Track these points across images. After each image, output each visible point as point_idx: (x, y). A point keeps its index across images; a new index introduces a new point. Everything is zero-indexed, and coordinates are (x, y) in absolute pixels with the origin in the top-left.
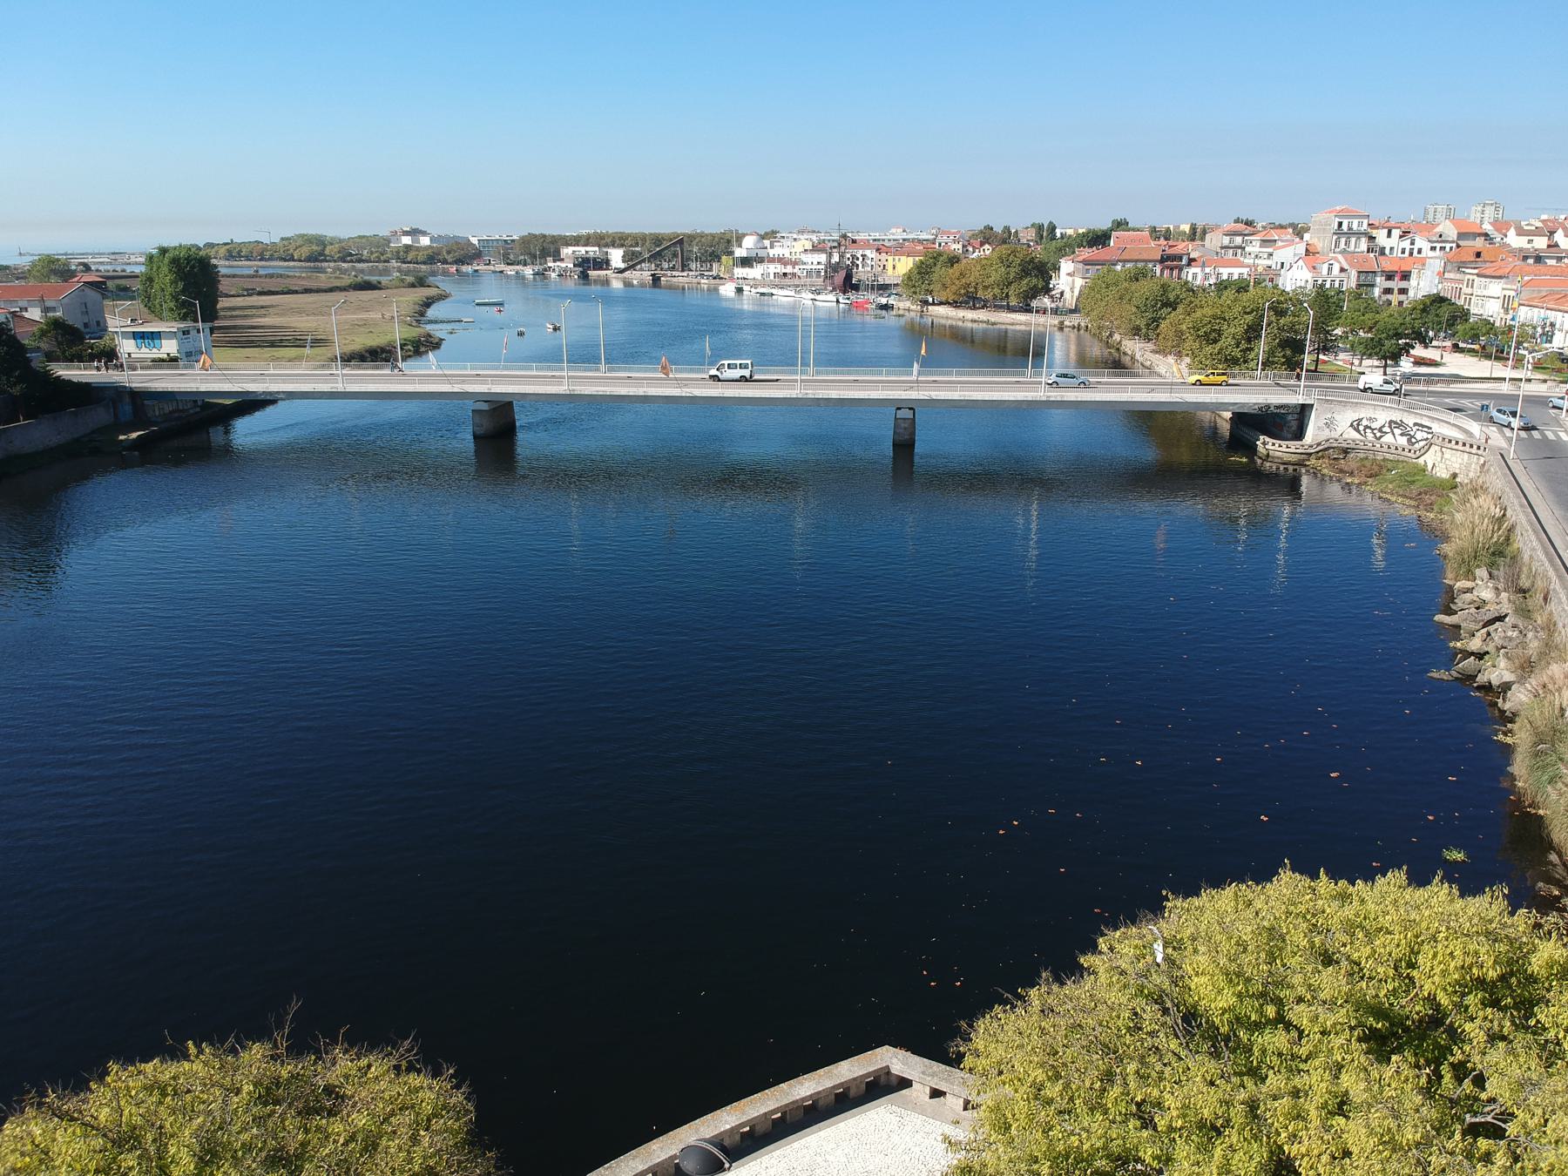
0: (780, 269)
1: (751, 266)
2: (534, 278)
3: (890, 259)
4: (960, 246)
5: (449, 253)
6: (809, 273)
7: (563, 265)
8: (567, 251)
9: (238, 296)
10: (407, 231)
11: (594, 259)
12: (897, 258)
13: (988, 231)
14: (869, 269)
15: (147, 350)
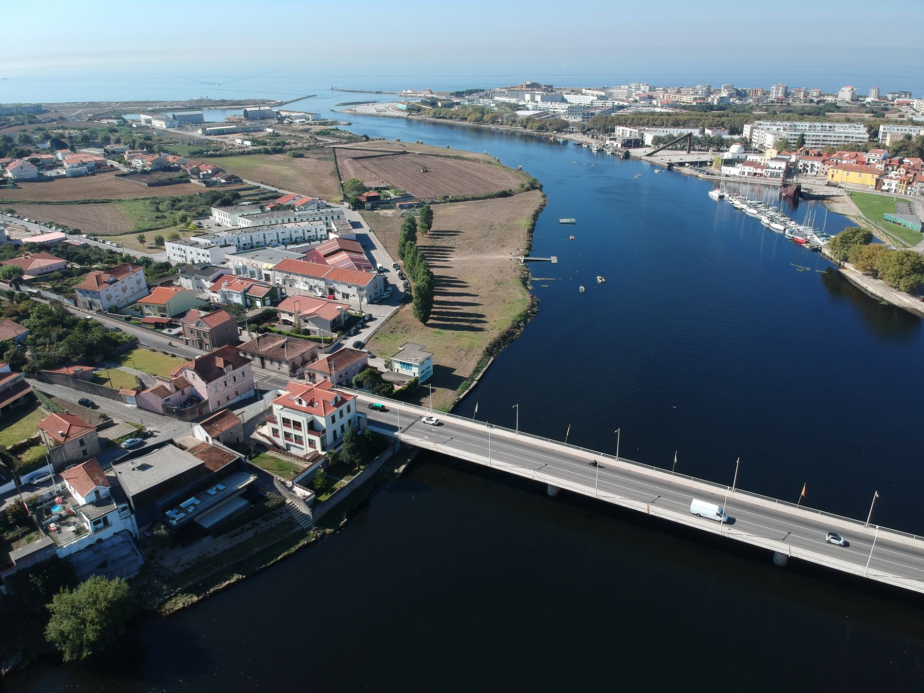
0: (752, 170)
1: (733, 165)
2: (597, 153)
3: (831, 170)
4: (883, 166)
6: (772, 175)
8: (619, 130)
9: (440, 203)
10: (528, 85)
11: (635, 140)
12: (835, 170)
14: (815, 173)
15: (405, 369)
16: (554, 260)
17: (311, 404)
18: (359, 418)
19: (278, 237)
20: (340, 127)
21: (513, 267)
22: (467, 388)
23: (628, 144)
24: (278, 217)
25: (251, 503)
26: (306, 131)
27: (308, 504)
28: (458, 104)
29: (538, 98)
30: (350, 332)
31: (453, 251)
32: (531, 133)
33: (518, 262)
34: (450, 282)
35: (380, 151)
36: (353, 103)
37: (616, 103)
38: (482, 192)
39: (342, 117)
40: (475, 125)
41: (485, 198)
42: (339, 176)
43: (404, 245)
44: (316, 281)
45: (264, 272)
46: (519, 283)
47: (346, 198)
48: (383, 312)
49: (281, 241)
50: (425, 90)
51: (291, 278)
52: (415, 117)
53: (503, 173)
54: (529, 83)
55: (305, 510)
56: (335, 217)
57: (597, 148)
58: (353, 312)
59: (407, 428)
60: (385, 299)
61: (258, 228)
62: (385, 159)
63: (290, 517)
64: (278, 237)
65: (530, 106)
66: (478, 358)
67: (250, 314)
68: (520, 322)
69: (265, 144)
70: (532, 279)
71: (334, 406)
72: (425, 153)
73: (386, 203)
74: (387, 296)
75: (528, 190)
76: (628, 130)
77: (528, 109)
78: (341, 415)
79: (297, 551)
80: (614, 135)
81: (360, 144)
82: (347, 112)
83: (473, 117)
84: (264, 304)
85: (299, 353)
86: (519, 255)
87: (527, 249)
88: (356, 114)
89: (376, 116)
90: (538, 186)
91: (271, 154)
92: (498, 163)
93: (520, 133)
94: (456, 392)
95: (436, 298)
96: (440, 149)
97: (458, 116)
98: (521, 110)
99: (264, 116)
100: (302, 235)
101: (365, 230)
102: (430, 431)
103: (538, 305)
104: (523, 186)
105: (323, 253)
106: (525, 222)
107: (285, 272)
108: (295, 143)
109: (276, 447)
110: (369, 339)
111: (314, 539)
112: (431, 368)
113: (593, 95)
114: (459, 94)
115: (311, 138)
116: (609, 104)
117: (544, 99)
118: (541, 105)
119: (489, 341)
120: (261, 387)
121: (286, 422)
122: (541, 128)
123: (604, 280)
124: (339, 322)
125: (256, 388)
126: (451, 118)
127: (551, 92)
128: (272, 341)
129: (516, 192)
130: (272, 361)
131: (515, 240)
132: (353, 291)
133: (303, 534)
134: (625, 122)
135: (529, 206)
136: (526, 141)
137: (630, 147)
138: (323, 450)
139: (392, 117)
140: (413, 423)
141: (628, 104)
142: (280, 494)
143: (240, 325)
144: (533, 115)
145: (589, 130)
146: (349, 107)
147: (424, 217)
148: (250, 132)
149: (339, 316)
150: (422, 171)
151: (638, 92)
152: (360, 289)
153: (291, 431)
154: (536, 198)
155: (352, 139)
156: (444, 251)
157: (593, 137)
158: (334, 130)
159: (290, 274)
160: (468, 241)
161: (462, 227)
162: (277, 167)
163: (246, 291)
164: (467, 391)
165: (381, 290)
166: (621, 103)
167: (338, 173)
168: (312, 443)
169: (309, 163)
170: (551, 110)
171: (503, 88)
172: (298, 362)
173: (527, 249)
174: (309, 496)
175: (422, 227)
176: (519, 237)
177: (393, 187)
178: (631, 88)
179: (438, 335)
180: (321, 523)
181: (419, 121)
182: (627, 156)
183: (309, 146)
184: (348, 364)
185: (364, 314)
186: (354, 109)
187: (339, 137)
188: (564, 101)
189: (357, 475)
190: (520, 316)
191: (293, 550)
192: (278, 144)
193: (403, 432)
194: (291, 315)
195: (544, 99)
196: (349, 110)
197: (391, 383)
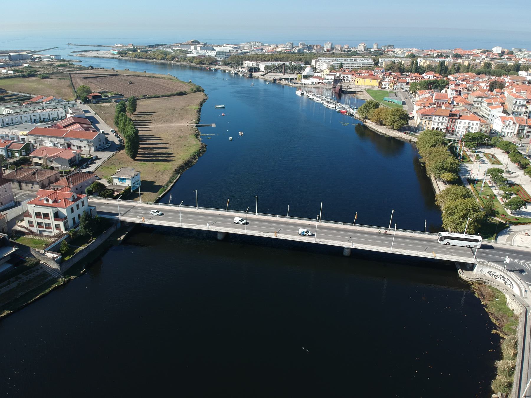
2: (234, 76)
3: (357, 79)
4: (382, 76)
5: (207, 61)
7: (244, 70)
8: (246, 63)
9: (141, 99)
10: (192, 42)
12: (359, 79)
13: (393, 64)
15: (122, 183)
16: (214, 125)
17: (55, 201)
18: (91, 209)
19: (31, 118)
20: (74, 63)
21: (189, 129)
22: (164, 191)
23: (251, 70)
24: (31, 108)
25: (15, 266)
26: (51, 65)
27: (57, 261)
28: (150, 50)
29: (199, 48)
30: (83, 166)
31: (151, 122)
32: (195, 66)
33: (192, 127)
34: (149, 138)
35: (101, 74)
36: (82, 51)
37: (243, 51)
38: (168, 93)
39: (75, 58)
40: (162, 61)
41: (170, 96)
42: (74, 87)
43: (118, 117)
44: (57, 139)
45: (21, 137)
46: (193, 136)
47: (78, 97)
48: (104, 156)
49: (33, 121)
50: (130, 44)
51: (40, 139)
52: (123, 57)
53: (180, 84)
54: (193, 41)
55: (54, 266)
56: (71, 106)
57: (234, 72)
58: (85, 156)
59: (125, 214)
60: (107, 148)
61: (16, 113)
62: (104, 78)
63: (44, 272)
64: (31, 118)
65: (194, 52)
66: (171, 175)
67: (11, 161)
68: (195, 156)
69: (23, 72)
70: (201, 135)
71: (72, 201)
72: (130, 75)
73: (105, 100)
74: (108, 147)
75: (196, 92)
76: (251, 63)
77: (193, 53)
78: (78, 208)
79: (50, 292)
80: (243, 66)
81: (87, 71)
82: (78, 55)
83: (160, 57)
84: (21, 154)
85: (46, 177)
86: (193, 123)
87: (197, 120)
88: (84, 57)
89: (98, 57)
90: (202, 90)
91: (26, 77)
92: (176, 79)
93: (189, 66)
94: (157, 194)
95: (141, 146)
96: (141, 73)
97: (151, 56)
98: (189, 54)
99: (22, 58)
100: (48, 117)
101: (92, 113)
102: (141, 213)
103: (205, 147)
104: (192, 89)
105: (62, 125)
106: (195, 107)
107: (36, 135)
108: (43, 71)
109: (31, 233)
110: (96, 169)
111: (62, 283)
112: (139, 182)
113: (230, 47)
114: (150, 46)
115: (54, 68)
116: (240, 51)
117: (202, 48)
118: (200, 51)
119: (177, 166)
120: (19, 200)
121: (38, 215)
122: (201, 63)
123: (243, 134)
124: (74, 161)
125: (16, 201)
126: (146, 58)
127: (206, 46)
128: (27, 172)
129: (188, 93)
130: (26, 183)
131: (190, 116)
132: (84, 144)
133: (55, 281)
134: (248, 59)
135: (196, 100)
136: (193, 69)
137: (252, 72)
138: (66, 230)
139: (109, 58)
140: (129, 211)
141: (250, 51)
142: (35, 257)
143: (4, 167)
144: (196, 56)
145: (229, 64)
146: (80, 53)
147: (131, 104)
148: (13, 66)
149: (75, 157)
150: (129, 83)
151: (255, 46)
152: (89, 143)
153: (43, 220)
154: (201, 96)
155: (81, 68)
156: (145, 123)
157: (231, 67)
158: (70, 64)
159: (39, 136)
160: (160, 117)
161: (156, 110)
162: (30, 84)
163: (7, 147)
164: (164, 193)
165: (103, 143)
166: (246, 51)
167: (73, 86)
168: (57, 227)
169: (53, 81)
170: (206, 55)
171: (177, 43)
172: (46, 183)
173: (197, 120)
174: (57, 257)
175: (130, 110)
176: (192, 114)
177: (110, 92)
178: (251, 44)
179: (143, 165)
180: (66, 273)
181: (126, 60)
182: (251, 76)
183: (53, 72)
184: (82, 181)
185: (92, 156)
186: (83, 54)
187: (74, 68)
188: (213, 50)
189: (90, 244)
190: (195, 152)
191: (47, 291)
192: (31, 72)
193: (122, 216)
194: (40, 159)
195: (202, 48)
196: (80, 54)
197: (113, 191)
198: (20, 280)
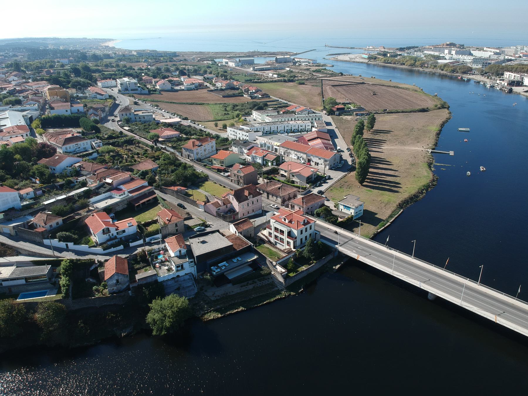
5: (460, 69)
7: (503, 83)
8: (507, 75)
10: (448, 44)
11: (517, 81)
16: (452, 153)
17: (290, 222)
18: (316, 234)
19: (284, 128)
20: (327, 68)
21: (423, 156)
22: (383, 226)
23: (512, 83)
24: (286, 117)
25: (254, 270)
26: (308, 70)
27: (283, 276)
28: (400, 55)
29: (453, 52)
30: (316, 185)
32: (445, 74)
33: (427, 153)
34: (381, 161)
35: (348, 82)
36: (336, 54)
38: (409, 109)
39: (329, 62)
40: (410, 68)
41: (411, 112)
42: (323, 95)
43: (355, 137)
44: (301, 154)
45: (275, 147)
46: (426, 165)
47: (325, 108)
48: (337, 175)
49: (286, 130)
50: (380, 47)
51: (288, 151)
52: (372, 62)
53: (424, 97)
54: (448, 43)
55: (281, 280)
56: (317, 119)
57: (490, 85)
58: (320, 174)
59: (343, 244)
60: (339, 167)
61: (274, 123)
62: (351, 86)
63: (273, 282)
64: (284, 128)
65: (447, 57)
66: (393, 209)
67: (265, 169)
68: (423, 190)
69: (285, 76)
70: (435, 164)
71: (303, 225)
72: (375, 84)
73: (347, 112)
74: (341, 166)
75: (439, 108)
76: (513, 74)
77: (445, 59)
78: (306, 231)
79: (274, 301)
80: (503, 77)
81: (337, 77)
82: (332, 59)
83: (409, 63)
84: (272, 165)
85: (287, 193)
86: (429, 148)
87: (434, 145)
88: (337, 61)
89: (349, 61)
90: (447, 106)
91: (287, 82)
92: (421, 91)
93: (438, 74)
94: (376, 228)
95: (371, 170)
96: (385, 81)
97: (399, 62)
98: (441, 59)
99: (286, 61)
100: (298, 128)
101: (333, 127)
102: (357, 248)
103: (437, 180)
104: (436, 106)
105: (307, 139)
106: (434, 128)
107: (286, 148)
108: (300, 76)
109: (270, 242)
110: (327, 189)
111: (284, 296)
112: (362, 211)
113: (491, 52)
114: (401, 49)
115: (310, 73)
117: (457, 53)
118: (455, 56)
119: (401, 199)
120: (266, 209)
121: (276, 229)
122: (453, 71)
123: (485, 169)
124: (311, 178)
125: (263, 209)
126: (395, 63)
127: (463, 49)
128: (274, 185)
129: (431, 110)
130: (273, 195)
131: (427, 139)
132: (321, 161)
133: (279, 292)
134: (511, 69)
135: (438, 119)
136: (442, 78)
137: (513, 85)
138: (294, 248)
139: (358, 62)
140: (347, 242)
142: (269, 268)
143: (259, 174)
144: (449, 62)
145: (486, 73)
146: (334, 56)
147: (370, 121)
148: (278, 69)
149: (312, 175)
150: (372, 94)
152: (325, 161)
153: (278, 235)
154: (444, 114)
155: (333, 75)
156: (380, 142)
157: (488, 78)
158: (323, 69)
159: (288, 149)
160: (396, 137)
161: (393, 128)
162: (289, 90)
163: (264, 157)
164: (383, 228)
165: (337, 162)
167: (322, 94)
168: (288, 243)
169: (307, 88)
170: (461, 60)
171: (431, 46)
172: (286, 198)
173: (434, 145)
174: (284, 272)
175: (368, 127)
176: (429, 137)
177: (353, 103)
179: (369, 192)
181: (374, 65)
182: (511, 91)
183: (308, 78)
184: (313, 203)
185: (325, 175)
186: (337, 57)
187: (326, 73)
188: (471, 54)
189: (311, 266)
190: (424, 186)
191: (272, 300)
192: (291, 77)
193: (340, 246)
194: (286, 172)
195: (457, 53)
196: (334, 58)
197: (337, 217)
198: (255, 284)
